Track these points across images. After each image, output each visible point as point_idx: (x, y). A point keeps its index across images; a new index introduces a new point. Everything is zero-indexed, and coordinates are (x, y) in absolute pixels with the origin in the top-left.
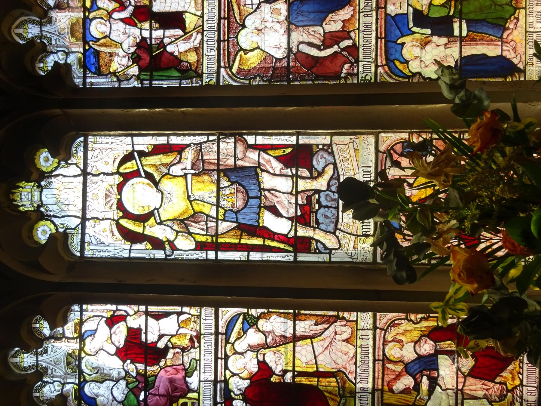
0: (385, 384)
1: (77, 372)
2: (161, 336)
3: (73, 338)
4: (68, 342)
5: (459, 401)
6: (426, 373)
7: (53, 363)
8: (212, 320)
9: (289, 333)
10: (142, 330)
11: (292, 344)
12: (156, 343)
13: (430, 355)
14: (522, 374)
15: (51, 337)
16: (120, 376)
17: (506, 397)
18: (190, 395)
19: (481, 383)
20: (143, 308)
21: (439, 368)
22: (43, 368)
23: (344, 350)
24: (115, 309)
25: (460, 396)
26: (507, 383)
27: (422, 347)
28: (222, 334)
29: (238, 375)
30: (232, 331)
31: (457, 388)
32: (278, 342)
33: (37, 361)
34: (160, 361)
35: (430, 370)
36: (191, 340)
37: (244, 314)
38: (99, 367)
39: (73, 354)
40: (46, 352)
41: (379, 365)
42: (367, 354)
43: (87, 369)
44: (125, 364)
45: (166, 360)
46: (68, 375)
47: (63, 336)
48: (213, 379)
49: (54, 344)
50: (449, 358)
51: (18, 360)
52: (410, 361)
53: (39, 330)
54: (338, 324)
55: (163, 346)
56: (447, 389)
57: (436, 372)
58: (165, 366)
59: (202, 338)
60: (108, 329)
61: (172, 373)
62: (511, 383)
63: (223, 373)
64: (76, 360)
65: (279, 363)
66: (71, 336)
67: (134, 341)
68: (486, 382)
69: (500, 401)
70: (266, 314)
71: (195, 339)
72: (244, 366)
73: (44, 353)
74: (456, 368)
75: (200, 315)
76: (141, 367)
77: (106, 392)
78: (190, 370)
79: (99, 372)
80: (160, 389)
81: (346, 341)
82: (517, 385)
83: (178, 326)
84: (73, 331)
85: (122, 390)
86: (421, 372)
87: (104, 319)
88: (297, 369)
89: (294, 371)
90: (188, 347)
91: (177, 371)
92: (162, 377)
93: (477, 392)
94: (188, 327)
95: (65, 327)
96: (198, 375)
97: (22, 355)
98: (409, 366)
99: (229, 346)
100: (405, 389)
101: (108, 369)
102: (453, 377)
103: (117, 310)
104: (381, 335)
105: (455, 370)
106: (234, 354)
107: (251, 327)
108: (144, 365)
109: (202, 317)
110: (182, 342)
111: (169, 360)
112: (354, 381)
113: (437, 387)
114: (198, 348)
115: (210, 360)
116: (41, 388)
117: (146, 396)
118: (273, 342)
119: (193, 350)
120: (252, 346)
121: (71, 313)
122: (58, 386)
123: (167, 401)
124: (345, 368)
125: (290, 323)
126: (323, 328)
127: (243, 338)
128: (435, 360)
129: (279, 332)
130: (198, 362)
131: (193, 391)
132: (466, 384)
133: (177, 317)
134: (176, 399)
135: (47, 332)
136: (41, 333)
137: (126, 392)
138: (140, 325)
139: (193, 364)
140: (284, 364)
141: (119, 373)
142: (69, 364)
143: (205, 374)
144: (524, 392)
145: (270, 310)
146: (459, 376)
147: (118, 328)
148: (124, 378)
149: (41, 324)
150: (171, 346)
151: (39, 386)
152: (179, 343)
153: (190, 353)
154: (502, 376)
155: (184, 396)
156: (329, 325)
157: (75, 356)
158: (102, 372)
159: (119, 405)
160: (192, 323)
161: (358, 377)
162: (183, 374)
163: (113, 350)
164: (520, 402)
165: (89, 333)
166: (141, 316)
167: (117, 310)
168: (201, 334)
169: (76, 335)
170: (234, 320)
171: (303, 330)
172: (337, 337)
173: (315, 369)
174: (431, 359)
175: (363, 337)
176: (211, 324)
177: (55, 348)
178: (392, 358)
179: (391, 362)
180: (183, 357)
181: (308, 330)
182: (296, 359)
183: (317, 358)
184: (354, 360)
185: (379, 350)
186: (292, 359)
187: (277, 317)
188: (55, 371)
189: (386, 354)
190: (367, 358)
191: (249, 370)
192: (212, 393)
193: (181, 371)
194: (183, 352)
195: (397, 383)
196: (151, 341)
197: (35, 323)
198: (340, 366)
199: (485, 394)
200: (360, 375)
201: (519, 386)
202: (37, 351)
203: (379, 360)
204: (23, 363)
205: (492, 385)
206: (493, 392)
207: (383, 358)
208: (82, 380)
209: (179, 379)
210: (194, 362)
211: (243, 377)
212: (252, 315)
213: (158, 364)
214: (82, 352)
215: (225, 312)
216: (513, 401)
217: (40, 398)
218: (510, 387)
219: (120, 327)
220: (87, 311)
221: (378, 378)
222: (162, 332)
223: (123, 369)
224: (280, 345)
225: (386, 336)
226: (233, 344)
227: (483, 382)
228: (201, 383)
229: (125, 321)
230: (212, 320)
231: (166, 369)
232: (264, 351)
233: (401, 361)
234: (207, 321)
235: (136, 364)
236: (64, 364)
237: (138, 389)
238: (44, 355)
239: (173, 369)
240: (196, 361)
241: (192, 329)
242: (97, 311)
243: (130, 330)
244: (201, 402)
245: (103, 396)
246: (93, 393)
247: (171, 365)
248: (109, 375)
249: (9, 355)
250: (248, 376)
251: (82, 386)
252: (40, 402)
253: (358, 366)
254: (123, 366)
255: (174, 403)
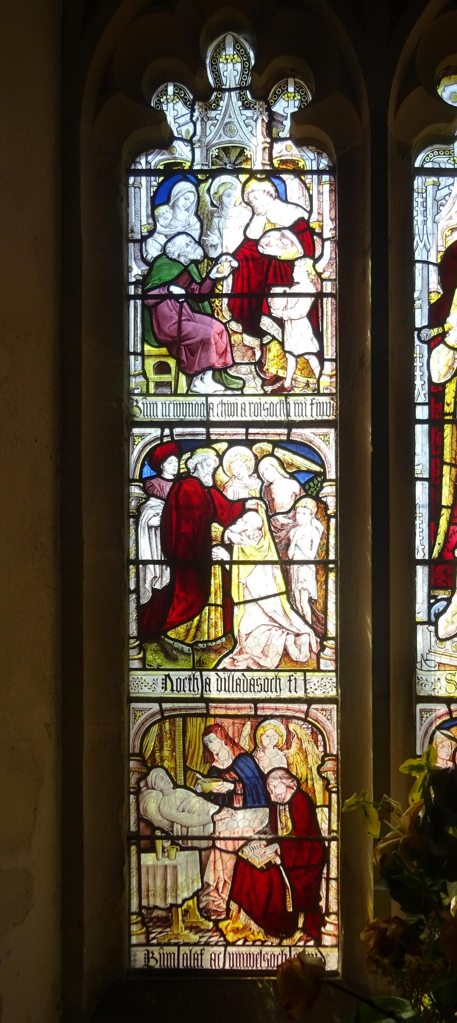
0: (218, 720)
1: (214, 167)
2: (280, 322)
3: (271, 158)
4: (264, 149)
5: (196, 843)
6: (238, 788)
7: (227, 120)
8: (312, 416)
9: (294, 553)
10: (290, 288)
11: (276, 558)
12: (270, 315)
13: (267, 795)
14: (243, 945)
15: (272, 116)
16: (209, 248)
17: (206, 919)
18: (183, 379)
19: (226, 878)
20: (328, 288)
21: (248, 810)
22: (218, 101)
23: (270, 650)
24: (325, 236)
25: (204, 844)
26: (229, 921)
27: (280, 780)
28: (289, 435)
29: (221, 464)
30: (295, 453)
31: (219, 839)
32: (278, 535)
33: (230, 90)
34: (238, 322)
35: (244, 794)
36: (277, 379)
37: (324, 474)
38: (222, 209)
39: (242, 158)
40: (246, 106)
41: (248, 709)
42: (266, 690)
43: (219, 186)
44: (230, 258)
45: (241, 334)
46: (207, 150)
47: (275, 140)
48: (212, 419)
49: (260, 121)
50: (264, 825)
51: (230, 51)
52: (256, 760)
53: (283, 91)
54: (314, 640)
55: (264, 328)
56: (214, 823)
57: (241, 804)
58: (230, 332)
59: (280, 398)
60: (289, 223)
61: (218, 345)
62: (229, 927)
63: (222, 438)
64: (234, 164)
65: (244, 538)
66: (275, 154)
67: (271, 274)
68: (229, 886)
69: (200, 910)
70: (326, 511)
71: (278, 385)
72: (236, 475)
73: (243, 102)
74: (251, 837)
75: (319, 394)
76: (227, 287)
77: (180, 223)
78: (226, 378)
79: (215, 209)
80: (192, 323)
81: (286, 653)
82: (227, 937)
83: (300, 353)
84: (283, 158)
85: (185, 252)
86: (240, 780)
87: (306, 216)
88: (235, 567)
89: (232, 562)
90: (264, 373)
91: (223, 354)
92: (211, 326)
93: (212, 872)
94: (298, 372)
95: (289, 143)
96: (217, 393)
97: (239, 60)
98: (249, 759)
99: (268, 447)
100: (211, 754)
101: (221, 226)
102: (234, 833)
103: (324, 241)
104: (297, 712)
105: (247, 835)
106: (255, 456)
107: (303, 486)
108: (229, 292)
109: (316, 398)
110: (273, 362)
111: (240, 338)
112: (220, 667)
113: (218, 807)
114: (262, 392)
115: (243, 414)
116: (182, 98)
117: (177, 297)
118: (278, 525)
119: (259, 382)
120: (270, 490)
121: (316, 153)
122: (188, 131)
123: (171, 337)
124: (240, 652)
125: (312, 555)
126: (305, 613)
127: (282, 472)
128: (260, 803)
129: (296, 535)
130: (240, 392)
131: (189, 384)
132: (224, 855)
133: (315, 351)
134: (174, 353)
135: (281, 107)
136: (277, 96)
137: (182, 260)
138: (298, 283)
139: (235, 383)
140: (243, 546)
141: (215, 246)
142: (226, 150)
143: (220, 406)
144: (215, 948)
145: (333, 521)
146: (236, 842)
147: (292, 242)
148: (206, 256)
149: (295, 96)
150: (264, 342)
151: (185, 95)
152: (270, 356)
153: (254, 378)
154: (239, 912)
155: (181, 368)
156: (310, 623)
157: (241, 163)
158: (216, 215)
159: (159, 247)
160: (305, 380)
161: (227, 674)
162: (218, 365)
163: (253, 234)
164: (199, 942)
165: (281, 188)
166: (315, 284)
167: (324, 241)
168: (286, 396)
169: (276, 163)
170: (313, 455)
171: (301, 579)
172: (291, 638)
173: (236, 600)
174: (262, 797)
175: (293, 682)
176: (304, 414)
177: (253, 124)
178: (260, 731)
179: (255, 729)
180: (246, 364)
181: (300, 586)
182: (252, 567)
183: (254, 603)
184: (255, 667)
185: (273, 709)
186: (251, 559)
187: (321, 531)
188: (212, 125)
189: (267, 722)
190: (259, 690)
191: (230, 483)
192: (188, 418)
193: (222, 361)
194: (255, 364)
195: (220, 741)
196: (272, 305)
197: (295, 83)
198: (245, 643)
199: (209, 885)
200: (231, 678)
201: (225, 940)
202: (246, 88)
203: (256, 709)
204: (225, 62)
205: (225, 896)
206: (213, 899)
207: (261, 716)
208: (200, 177)
209: (208, 358)
210: (238, 384)
211: (218, 472)
212: (322, 488)
213: (233, 318)
214: (248, 176)
215: (326, 439)
216: (201, 931)
217: (165, 97)
218: (222, 925)
219: (294, 247)
220: (320, 182)
221: (226, 708)
222: (287, 326)
223: (222, 255)
224: (273, 538)
225: (296, 721)
226: (272, 455)
227: (228, 881)
228: (204, 398)
229: (305, 256)
230: (312, 416)
231: (225, 333)
232: (262, 511)
233: (256, 745)
234: (309, 407)
235: (231, 276)
236: (225, 142)
237: (188, 282)
238: (240, 103)
239: (224, 347)
240: (242, 389)
241: (295, 381)
242: (320, 203)
243: (289, 265)
244: (173, 398)
245: (174, 217)
246: (178, 198)
247: (233, 342)
248: (209, 228)
249: (239, 33)
250: (219, 483)
251: (190, 176)
252: (158, 96)
253: (245, 673)
254: (227, 254)
255: (169, 350)
